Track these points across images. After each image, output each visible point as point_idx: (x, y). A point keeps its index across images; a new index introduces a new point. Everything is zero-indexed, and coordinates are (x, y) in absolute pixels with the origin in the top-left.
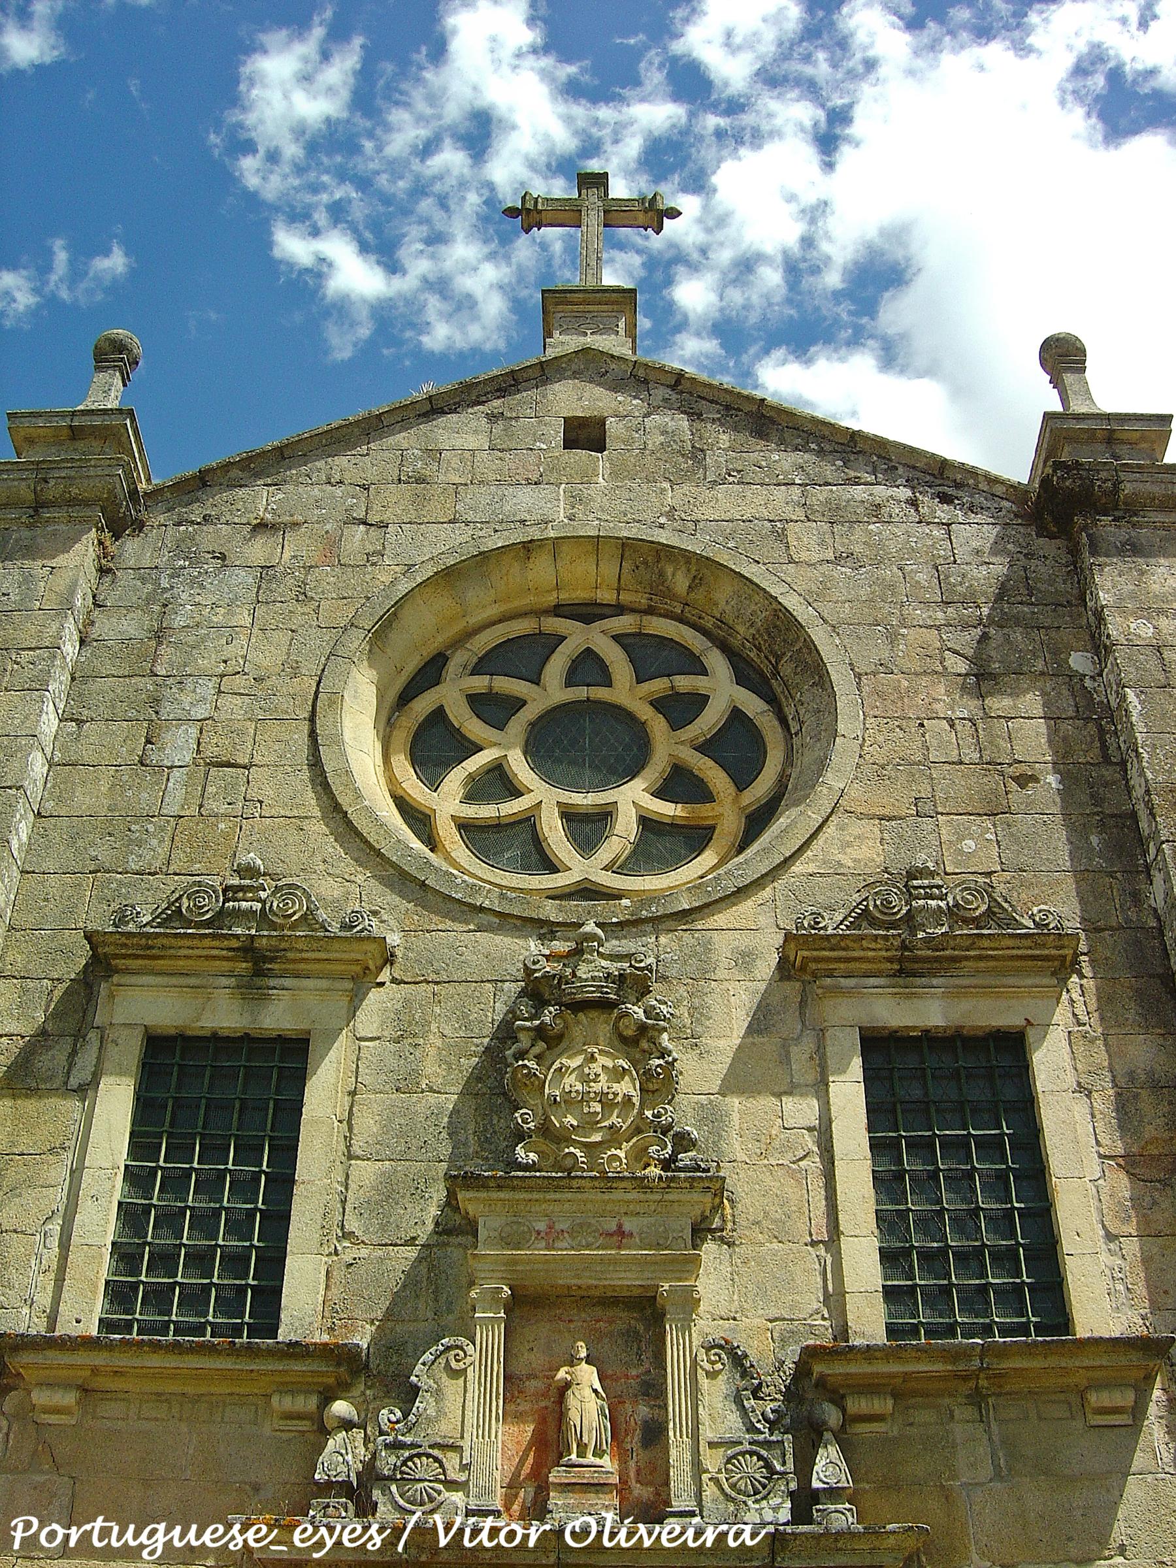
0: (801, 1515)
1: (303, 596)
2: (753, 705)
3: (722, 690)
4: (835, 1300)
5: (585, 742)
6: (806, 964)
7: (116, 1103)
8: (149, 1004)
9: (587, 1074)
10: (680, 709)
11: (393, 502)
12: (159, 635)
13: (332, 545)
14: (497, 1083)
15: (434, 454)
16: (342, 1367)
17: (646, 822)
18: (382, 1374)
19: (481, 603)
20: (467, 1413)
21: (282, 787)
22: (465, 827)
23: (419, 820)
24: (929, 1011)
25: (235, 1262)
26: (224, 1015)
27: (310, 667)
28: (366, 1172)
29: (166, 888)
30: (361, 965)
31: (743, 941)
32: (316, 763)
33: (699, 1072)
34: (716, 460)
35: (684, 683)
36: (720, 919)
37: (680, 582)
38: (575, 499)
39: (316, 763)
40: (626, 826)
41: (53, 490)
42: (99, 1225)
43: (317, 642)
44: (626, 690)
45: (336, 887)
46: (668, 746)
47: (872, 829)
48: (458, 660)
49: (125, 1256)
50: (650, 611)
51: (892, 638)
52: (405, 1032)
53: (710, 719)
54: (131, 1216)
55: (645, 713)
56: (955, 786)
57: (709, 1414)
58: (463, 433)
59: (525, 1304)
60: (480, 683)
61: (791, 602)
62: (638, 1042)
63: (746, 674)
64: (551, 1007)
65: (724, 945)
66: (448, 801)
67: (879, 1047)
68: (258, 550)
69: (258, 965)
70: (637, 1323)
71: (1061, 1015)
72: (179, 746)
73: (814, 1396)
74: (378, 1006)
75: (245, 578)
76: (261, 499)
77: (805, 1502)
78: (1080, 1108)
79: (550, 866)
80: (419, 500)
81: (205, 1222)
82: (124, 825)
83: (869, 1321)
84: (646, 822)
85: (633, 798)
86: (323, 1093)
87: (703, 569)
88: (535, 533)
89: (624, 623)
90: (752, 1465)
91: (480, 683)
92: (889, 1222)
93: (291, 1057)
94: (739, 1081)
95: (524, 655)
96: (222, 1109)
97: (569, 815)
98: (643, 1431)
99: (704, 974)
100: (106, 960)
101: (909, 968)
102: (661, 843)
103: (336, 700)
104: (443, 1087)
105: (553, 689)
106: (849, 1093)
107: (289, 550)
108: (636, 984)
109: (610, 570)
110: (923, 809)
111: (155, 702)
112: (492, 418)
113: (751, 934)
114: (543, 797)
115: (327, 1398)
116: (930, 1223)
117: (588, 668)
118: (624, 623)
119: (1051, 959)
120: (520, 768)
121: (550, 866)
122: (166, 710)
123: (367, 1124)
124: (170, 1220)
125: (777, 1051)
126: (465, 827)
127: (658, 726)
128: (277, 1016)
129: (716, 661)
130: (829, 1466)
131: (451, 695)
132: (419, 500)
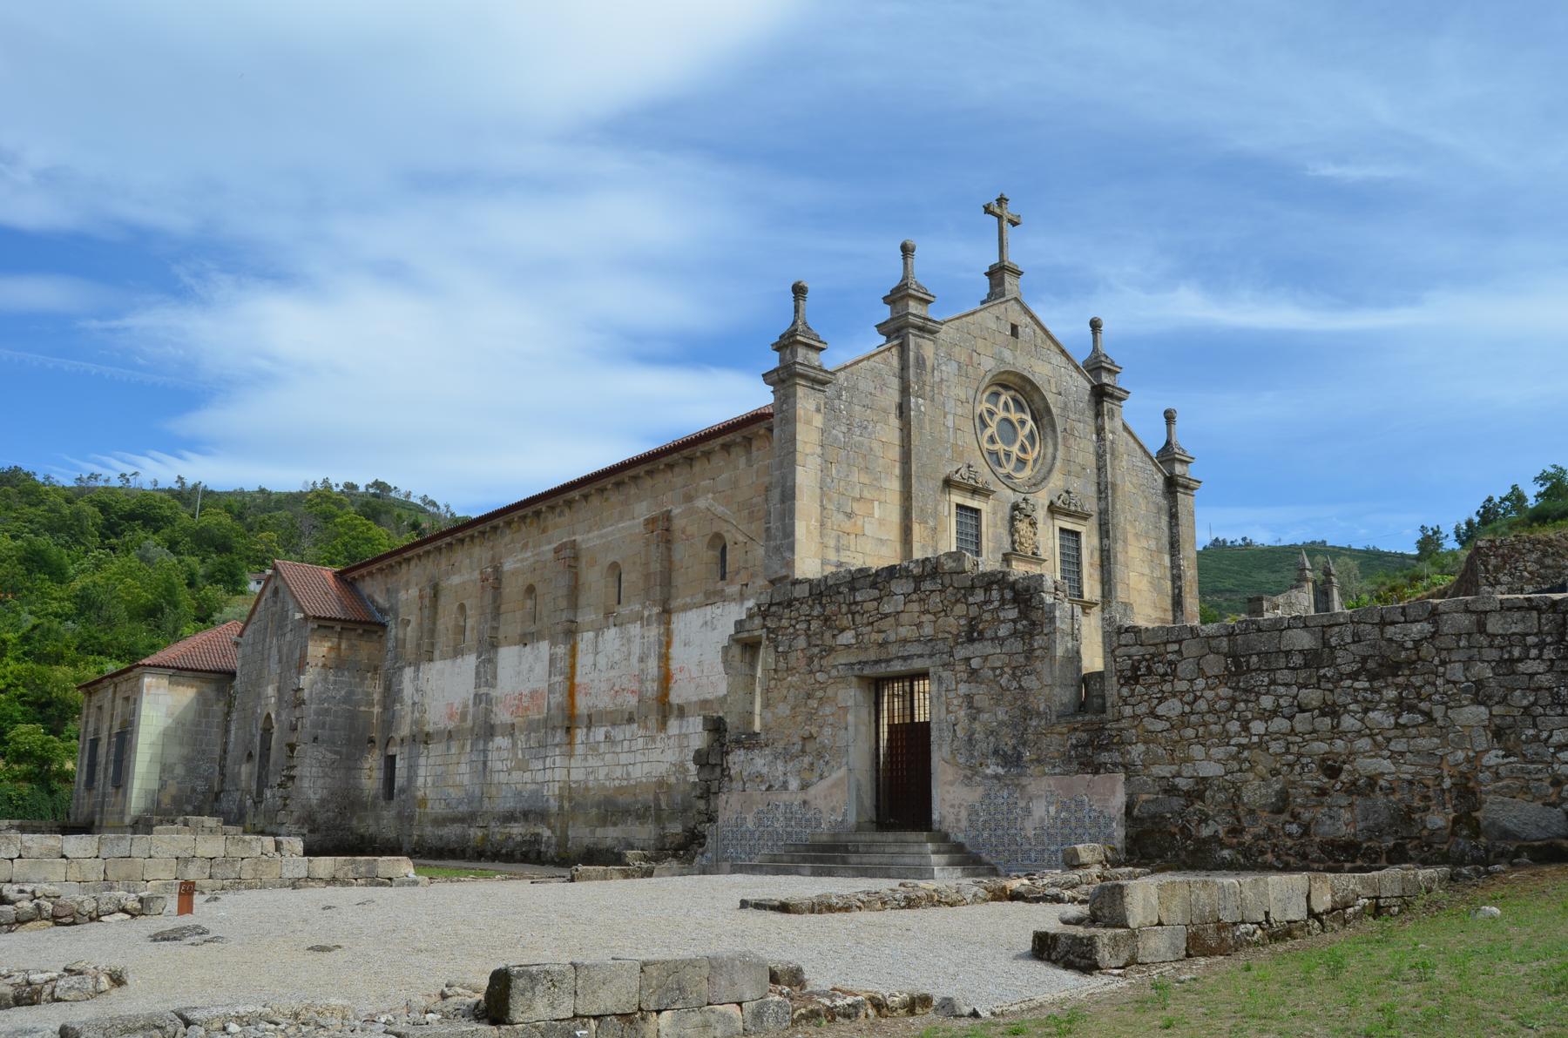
13: (971, 358)
24: (1069, 525)
40: (1014, 458)
43: (972, 393)
75: (955, 365)
88: (1008, 368)
101: (1069, 514)
118: (1012, 393)
119: (1084, 517)
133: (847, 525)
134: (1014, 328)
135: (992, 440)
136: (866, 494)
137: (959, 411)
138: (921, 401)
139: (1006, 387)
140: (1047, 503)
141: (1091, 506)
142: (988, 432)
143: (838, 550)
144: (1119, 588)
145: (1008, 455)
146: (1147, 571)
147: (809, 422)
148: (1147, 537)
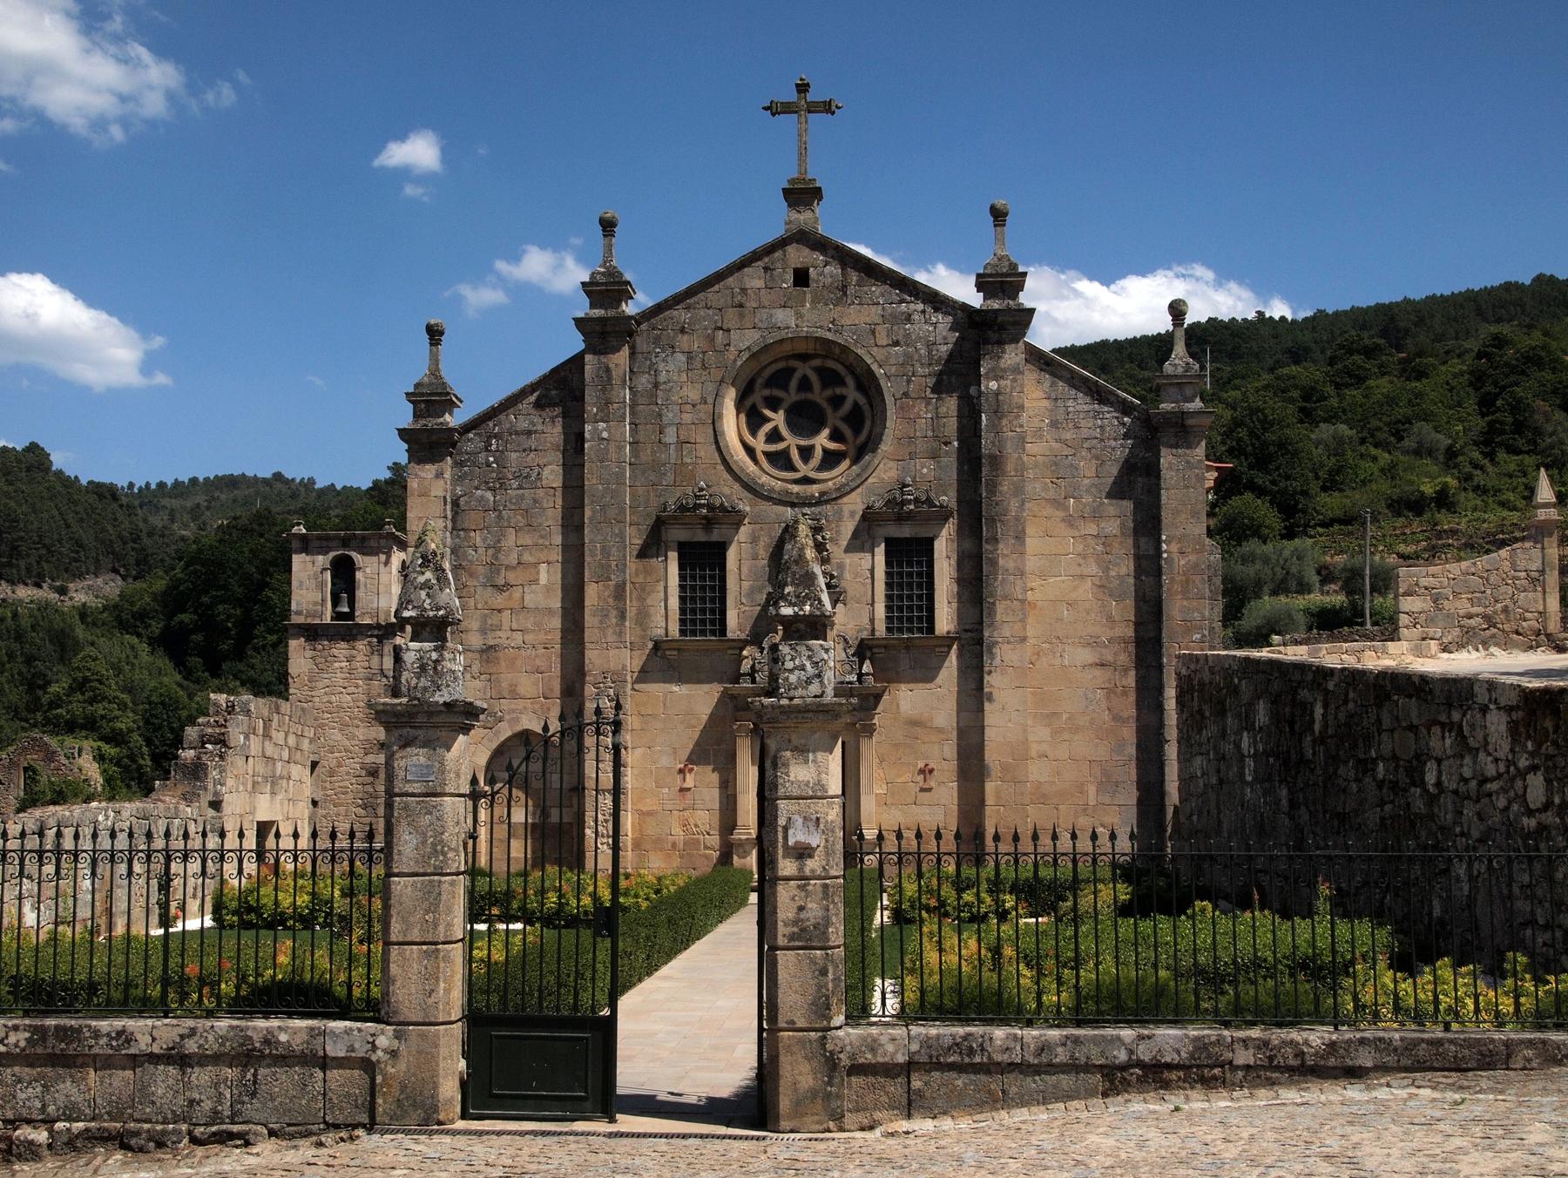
0: (860, 680)
1: (704, 367)
2: (862, 400)
3: (852, 394)
4: (872, 621)
5: (805, 418)
6: (869, 519)
8: (677, 534)
12: (656, 385)
13: (712, 339)
15: (744, 290)
17: (825, 450)
19: (765, 359)
21: (707, 452)
22: (766, 454)
23: (750, 451)
24: (906, 531)
25: (713, 611)
26: (701, 536)
27: (710, 400)
28: (746, 585)
30: (735, 518)
31: (852, 507)
32: (717, 442)
34: (851, 290)
35: (838, 391)
36: (845, 500)
37: (837, 351)
38: (799, 316)
39: (717, 442)
40: (818, 453)
41: (609, 329)
42: (674, 602)
43: (711, 387)
44: (819, 395)
45: (729, 492)
47: (892, 464)
48: (760, 381)
49: (683, 611)
50: (825, 357)
51: (909, 381)
52: (754, 540)
53: (847, 406)
54: (682, 599)
55: (824, 404)
56: (921, 446)
58: (754, 279)
60: (767, 392)
61: (874, 367)
63: (861, 387)
65: (846, 510)
66: (760, 444)
67: (890, 543)
68: (683, 341)
69: (708, 523)
71: (944, 532)
72: (670, 436)
73: (864, 649)
74: (744, 532)
75: (682, 358)
76: (680, 314)
77: (860, 675)
78: (946, 564)
79: (795, 470)
80: (742, 316)
81: (703, 611)
84: (825, 450)
86: (732, 555)
87: (845, 349)
88: (783, 334)
89: (817, 362)
90: (847, 667)
91: (767, 392)
92: (889, 597)
93: (721, 549)
94: (849, 549)
95: (780, 379)
97: (799, 448)
99: (840, 519)
101: (901, 518)
102: (831, 460)
103: (721, 416)
104: (764, 554)
105: (792, 396)
109: (811, 345)
110: (912, 456)
111: (660, 415)
112: (766, 269)
113: (854, 504)
114: (791, 442)
115: (742, 649)
116: (900, 597)
117: (805, 385)
118: (817, 362)
120: (784, 431)
121: (795, 470)
122: (665, 420)
123: (745, 570)
124: (693, 599)
125: (861, 541)
126: (766, 454)
127: (829, 411)
128: (715, 536)
129: (850, 381)
131: (756, 398)
132: (742, 316)
133: (499, 600)
134: (801, 278)
135: (774, 436)
136: (527, 558)
137: (687, 418)
138: (602, 425)
140: (860, 509)
141: (948, 499)
142: (767, 427)
143: (483, 631)
144: (1000, 608)
145: (806, 453)
146: (1093, 568)
147: (424, 494)
148: (1096, 516)
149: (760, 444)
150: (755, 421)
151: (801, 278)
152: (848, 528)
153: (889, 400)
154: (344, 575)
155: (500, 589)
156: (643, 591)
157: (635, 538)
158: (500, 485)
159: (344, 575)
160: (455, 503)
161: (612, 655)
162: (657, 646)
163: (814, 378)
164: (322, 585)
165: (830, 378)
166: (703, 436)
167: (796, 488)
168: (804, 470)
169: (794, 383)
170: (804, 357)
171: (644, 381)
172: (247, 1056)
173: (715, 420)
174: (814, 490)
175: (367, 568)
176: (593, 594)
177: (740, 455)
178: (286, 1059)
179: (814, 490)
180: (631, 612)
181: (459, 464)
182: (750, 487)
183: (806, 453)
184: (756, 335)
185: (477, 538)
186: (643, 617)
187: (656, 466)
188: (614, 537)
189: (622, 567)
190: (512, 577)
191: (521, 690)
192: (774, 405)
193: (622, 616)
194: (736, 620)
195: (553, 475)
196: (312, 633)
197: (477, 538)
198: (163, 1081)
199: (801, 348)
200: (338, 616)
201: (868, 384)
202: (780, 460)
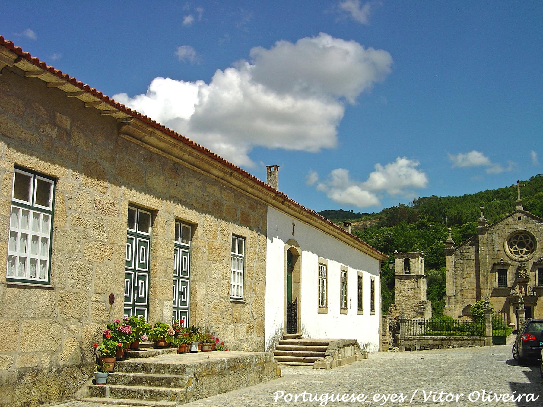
3: (530, 240)
7: (497, 273)
9: (522, 272)
10: (527, 242)
11: (506, 227)
14: (517, 272)
16: (511, 288)
18: (513, 288)
20: (517, 290)
23: (511, 251)
29: (497, 260)
30: (509, 265)
33: (528, 271)
42: (497, 281)
43: (503, 240)
44: (524, 240)
46: (527, 245)
53: (529, 243)
57: (529, 290)
59: (520, 284)
62: (525, 270)
63: (532, 239)
64: (520, 268)
66: (512, 250)
67: (538, 269)
68: (497, 232)
70: (525, 285)
72: (495, 249)
73: (534, 289)
82: (493, 255)
83: (537, 285)
85: (525, 249)
86: (508, 272)
93: (506, 270)
95: (516, 238)
96: (503, 273)
98: (526, 290)
100: (494, 266)
102: (526, 253)
105: (518, 241)
106: (537, 272)
107: (500, 232)
108: (525, 267)
113: (531, 261)
114: (519, 249)
117: (521, 239)
125: (533, 270)
130: (535, 293)
131: (512, 241)
133: (464, 280)
134: (520, 219)
135: (515, 249)
136: (469, 272)
139: (521, 233)
143: (461, 286)
145: (522, 252)
149: (512, 250)
150: (511, 245)
151: (520, 219)
152: (530, 266)
153: (537, 242)
154: (407, 264)
155: (464, 278)
156: (491, 278)
157: (489, 269)
158: (462, 259)
159: (407, 264)
160: (455, 263)
161: (486, 291)
162: (495, 289)
163: (523, 237)
164: (402, 266)
165: (526, 237)
166: (502, 249)
167: (520, 259)
168: (521, 255)
169: (519, 239)
170: (521, 233)
171: (490, 239)
172: (473, 340)
173: (504, 246)
174: (524, 259)
175: (413, 262)
176: (482, 279)
177: (509, 252)
178: (477, 340)
179: (524, 259)
180: (489, 283)
181: (455, 255)
182: (511, 259)
183: (522, 252)
184: (511, 230)
185: (459, 269)
186: (491, 283)
187: (493, 255)
188: (486, 268)
189: (487, 274)
190: (466, 276)
191: (468, 297)
192: (515, 242)
193: (487, 283)
194: (509, 284)
195: (473, 257)
196: (400, 278)
197: (459, 269)
198: (466, 342)
199: (520, 232)
200: (406, 273)
201: (533, 238)
202: (517, 253)
